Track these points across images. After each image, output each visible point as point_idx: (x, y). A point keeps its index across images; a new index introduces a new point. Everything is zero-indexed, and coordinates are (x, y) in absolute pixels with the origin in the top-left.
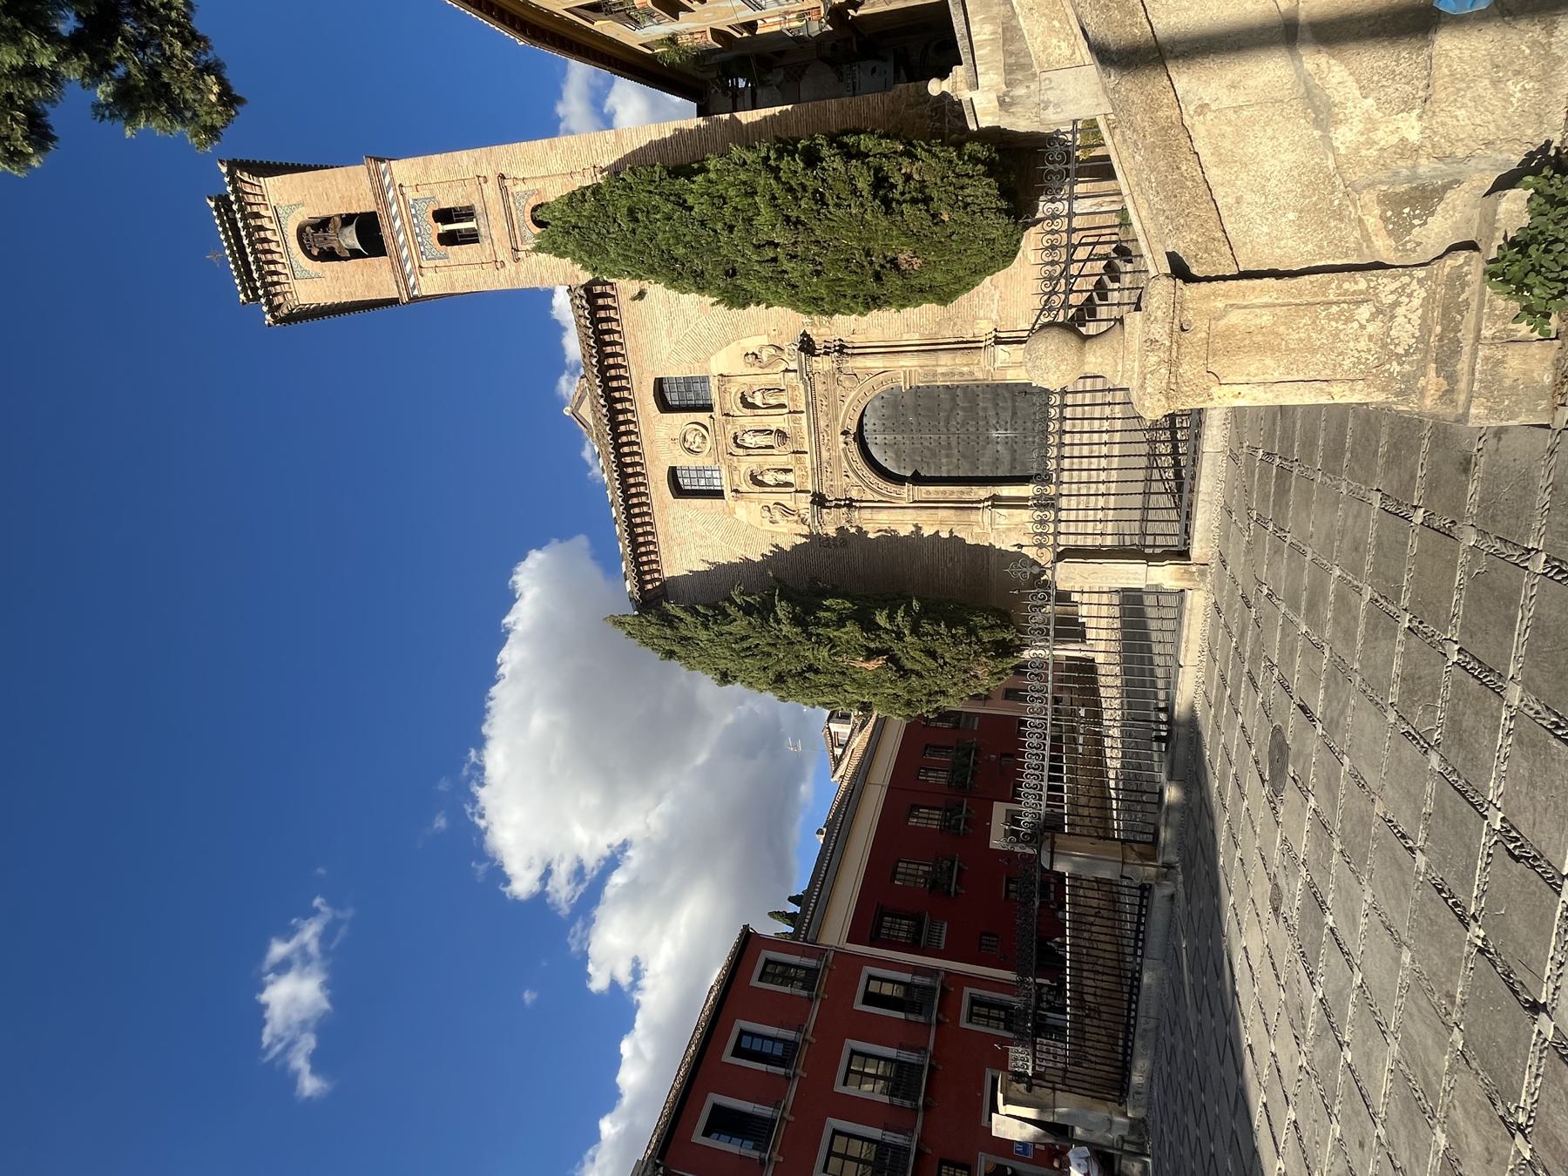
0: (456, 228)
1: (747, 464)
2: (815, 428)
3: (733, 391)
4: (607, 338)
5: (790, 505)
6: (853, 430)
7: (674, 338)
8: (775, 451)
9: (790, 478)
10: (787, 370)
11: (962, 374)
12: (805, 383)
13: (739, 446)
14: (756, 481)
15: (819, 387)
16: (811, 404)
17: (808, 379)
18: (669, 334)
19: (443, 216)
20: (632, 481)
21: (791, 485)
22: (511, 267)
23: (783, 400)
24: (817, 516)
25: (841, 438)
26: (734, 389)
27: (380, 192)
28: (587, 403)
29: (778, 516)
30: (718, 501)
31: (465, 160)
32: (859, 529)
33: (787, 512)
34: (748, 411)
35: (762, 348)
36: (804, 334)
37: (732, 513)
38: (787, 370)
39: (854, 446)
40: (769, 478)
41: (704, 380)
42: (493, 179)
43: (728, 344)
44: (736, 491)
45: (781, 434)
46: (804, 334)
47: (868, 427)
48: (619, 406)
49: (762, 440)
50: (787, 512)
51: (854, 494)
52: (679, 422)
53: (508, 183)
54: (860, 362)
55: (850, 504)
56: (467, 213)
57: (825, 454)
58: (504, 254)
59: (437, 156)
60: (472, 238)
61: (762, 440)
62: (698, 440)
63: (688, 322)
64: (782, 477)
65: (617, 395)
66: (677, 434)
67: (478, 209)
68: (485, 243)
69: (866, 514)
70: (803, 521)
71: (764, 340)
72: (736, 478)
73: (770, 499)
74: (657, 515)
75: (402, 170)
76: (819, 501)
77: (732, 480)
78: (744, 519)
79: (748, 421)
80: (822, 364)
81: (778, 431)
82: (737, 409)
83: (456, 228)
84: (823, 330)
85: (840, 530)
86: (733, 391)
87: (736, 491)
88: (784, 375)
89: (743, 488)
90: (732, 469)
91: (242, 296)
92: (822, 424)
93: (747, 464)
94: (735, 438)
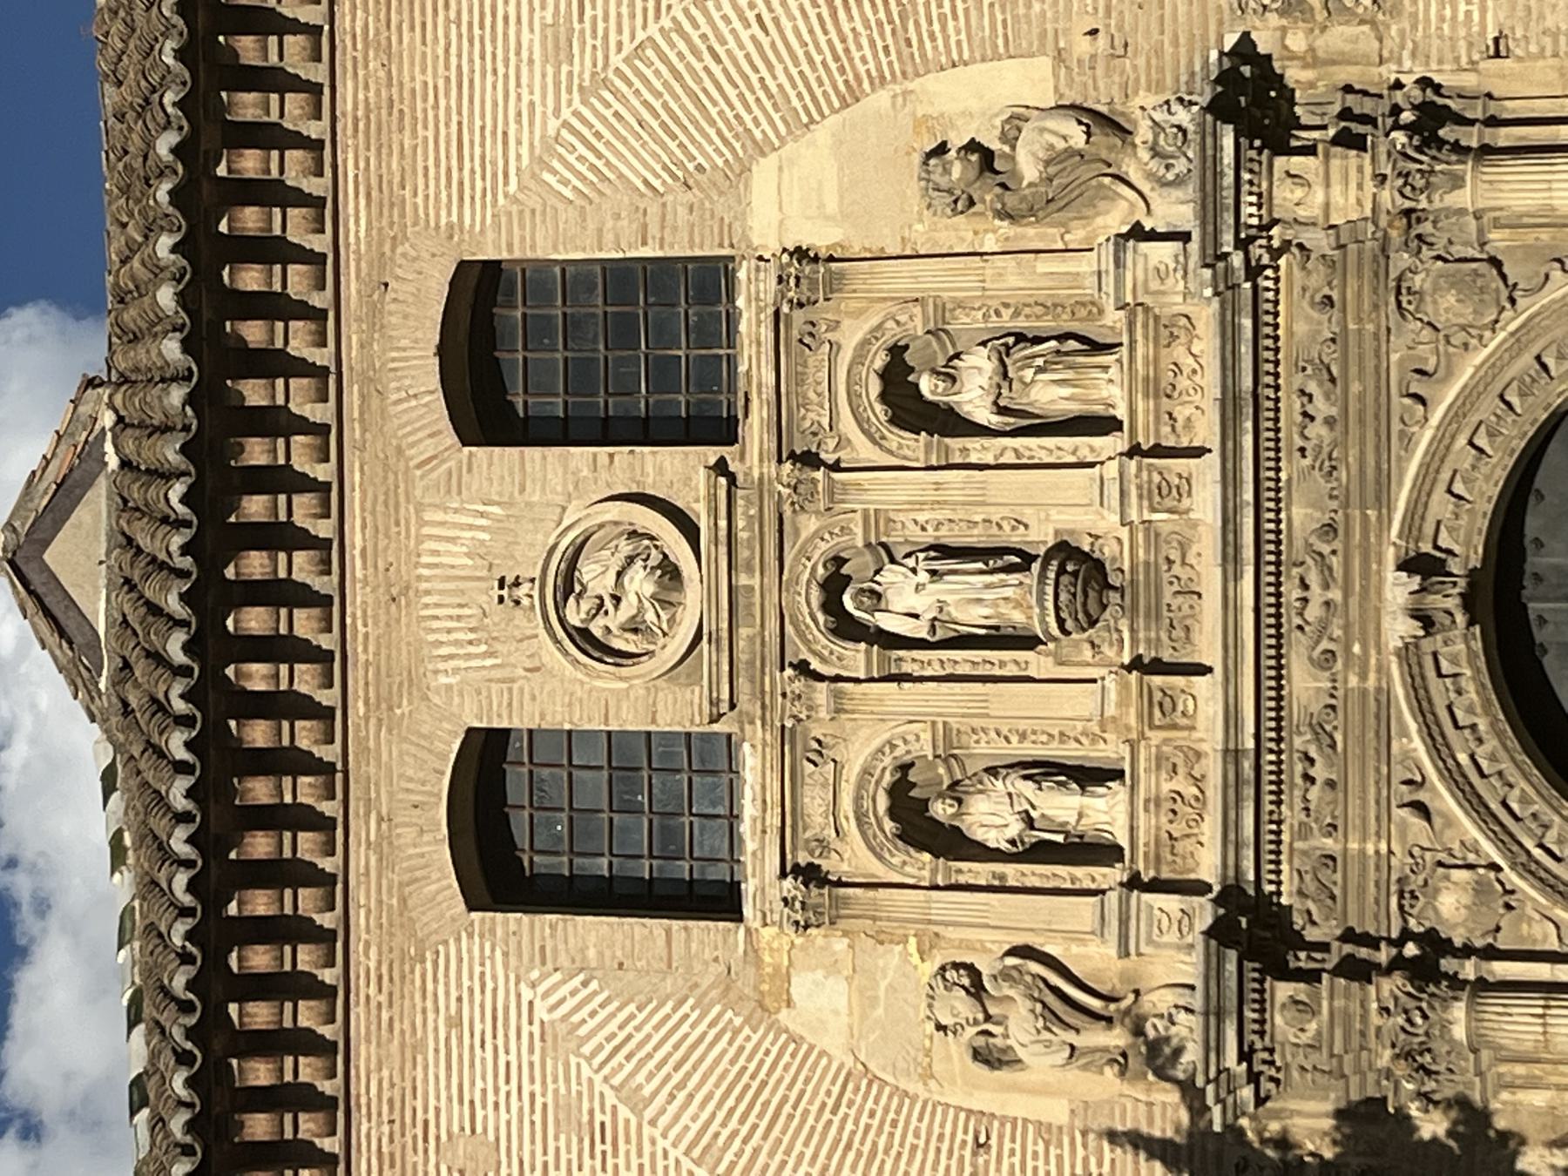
1: (883, 724)
2: (1261, 549)
3: (851, 336)
4: (247, 48)
5: (1093, 957)
6: (1465, 543)
7: (582, 66)
8: (1036, 662)
9: (1103, 812)
10: (1138, 233)
12: (1225, 289)
13: (847, 628)
14: (918, 819)
15: (1299, 323)
16: (1249, 404)
17: (1242, 257)
18: (560, 47)
20: (259, 790)
21: (1106, 853)
23: (1107, 388)
24: (1231, 1010)
25: (1398, 589)
26: (854, 332)
28: (94, 513)
29: (1019, 1025)
30: (703, 934)
32: (1472, 1117)
33: (1067, 999)
34: (915, 445)
35: (1014, 124)
36: (1245, 49)
37: (768, 1000)
38: (1138, 233)
39: (1461, 648)
40: (991, 817)
41: (709, 280)
43: (852, 96)
44: (811, 875)
45: (1080, 572)
46: (1245, 49)
47: (1553, 551)
48: (254, 393)
49: (974, 599)
50: (1067, 999)
51: (1451, 907)
52: (563, 489)
54: (1517, 189)
55: (1429, 962)
57: (1305, 685)
61: (974, 599)
62: (640, 583)
64: (1062, 807)
65: (253, 332)
66: (530, 557)
69: (1517, 1023)
70: (1157, 1057)
71: (1029, 81)
72: (815, 803)
73: (985, 924)
74: (366, 957)
76: (1253, 933)
77: (791, 819)
78: (833, 1042)
79: (907, 490)
80: (1323, 193)
81: (1064, 551)
82: (854, 429)
84: (1339, 37)
85: (1367, 1121)
86: (851, 336)
87: (811, 875)
88: (1130, 257)
89: (852, 857)
90: (796, 749)
92: (1301, 516)
93: (883, 724)
94: (834, 585)
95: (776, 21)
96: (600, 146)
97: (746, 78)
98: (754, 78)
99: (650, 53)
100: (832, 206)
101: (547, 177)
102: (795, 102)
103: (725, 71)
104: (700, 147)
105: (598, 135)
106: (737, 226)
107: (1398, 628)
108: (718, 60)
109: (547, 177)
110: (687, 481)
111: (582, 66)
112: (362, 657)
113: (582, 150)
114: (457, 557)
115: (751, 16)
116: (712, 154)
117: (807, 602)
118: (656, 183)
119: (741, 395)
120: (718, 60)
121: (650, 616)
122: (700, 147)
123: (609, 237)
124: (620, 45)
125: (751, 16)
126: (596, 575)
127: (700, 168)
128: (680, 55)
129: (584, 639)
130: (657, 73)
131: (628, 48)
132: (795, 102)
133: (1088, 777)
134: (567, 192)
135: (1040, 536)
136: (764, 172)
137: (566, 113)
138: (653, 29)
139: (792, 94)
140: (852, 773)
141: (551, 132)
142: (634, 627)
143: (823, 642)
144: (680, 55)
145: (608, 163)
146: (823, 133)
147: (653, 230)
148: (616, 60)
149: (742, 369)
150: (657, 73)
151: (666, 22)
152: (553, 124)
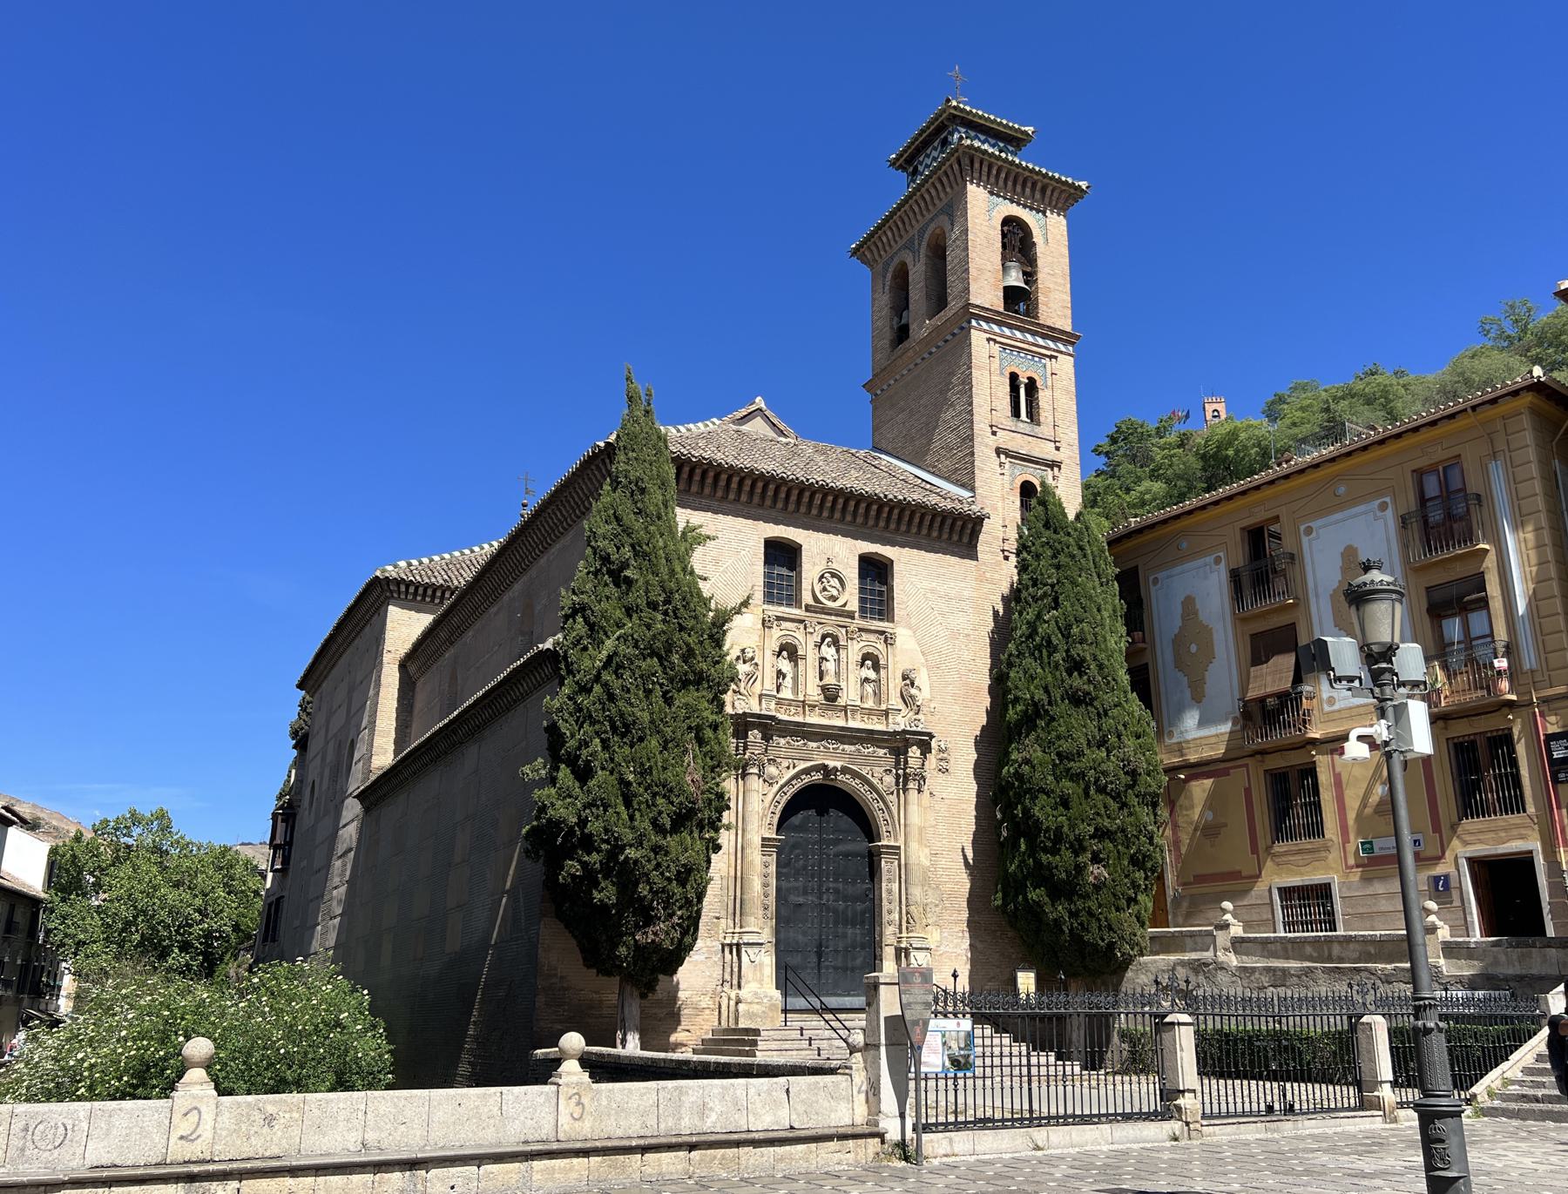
0: (1024, 396)
11: (890, 912)
13: (824, 637)
18: (933, 591)
19: (1032, 386)
22: (993, 442)
27: (1052, 334)
31: (1070, 434)
42: (1056, 456)
56: (1033, 415)
58: (1004, 439)
60: (1016, 413)
62: (835, 593)
67: (1037, 430)
68: (1010, 423)
75: (1065, 366)
83: (1024, 396)
91: (954, 103)
93: (807, 644)
107: (831, 764)
114: (837, 549)
116: (913, 621)
117: (829, 629)
126: (835, 582)
133: (795, 689)
135: (843, 684)
136: (910, 632)
142: (825, 589)
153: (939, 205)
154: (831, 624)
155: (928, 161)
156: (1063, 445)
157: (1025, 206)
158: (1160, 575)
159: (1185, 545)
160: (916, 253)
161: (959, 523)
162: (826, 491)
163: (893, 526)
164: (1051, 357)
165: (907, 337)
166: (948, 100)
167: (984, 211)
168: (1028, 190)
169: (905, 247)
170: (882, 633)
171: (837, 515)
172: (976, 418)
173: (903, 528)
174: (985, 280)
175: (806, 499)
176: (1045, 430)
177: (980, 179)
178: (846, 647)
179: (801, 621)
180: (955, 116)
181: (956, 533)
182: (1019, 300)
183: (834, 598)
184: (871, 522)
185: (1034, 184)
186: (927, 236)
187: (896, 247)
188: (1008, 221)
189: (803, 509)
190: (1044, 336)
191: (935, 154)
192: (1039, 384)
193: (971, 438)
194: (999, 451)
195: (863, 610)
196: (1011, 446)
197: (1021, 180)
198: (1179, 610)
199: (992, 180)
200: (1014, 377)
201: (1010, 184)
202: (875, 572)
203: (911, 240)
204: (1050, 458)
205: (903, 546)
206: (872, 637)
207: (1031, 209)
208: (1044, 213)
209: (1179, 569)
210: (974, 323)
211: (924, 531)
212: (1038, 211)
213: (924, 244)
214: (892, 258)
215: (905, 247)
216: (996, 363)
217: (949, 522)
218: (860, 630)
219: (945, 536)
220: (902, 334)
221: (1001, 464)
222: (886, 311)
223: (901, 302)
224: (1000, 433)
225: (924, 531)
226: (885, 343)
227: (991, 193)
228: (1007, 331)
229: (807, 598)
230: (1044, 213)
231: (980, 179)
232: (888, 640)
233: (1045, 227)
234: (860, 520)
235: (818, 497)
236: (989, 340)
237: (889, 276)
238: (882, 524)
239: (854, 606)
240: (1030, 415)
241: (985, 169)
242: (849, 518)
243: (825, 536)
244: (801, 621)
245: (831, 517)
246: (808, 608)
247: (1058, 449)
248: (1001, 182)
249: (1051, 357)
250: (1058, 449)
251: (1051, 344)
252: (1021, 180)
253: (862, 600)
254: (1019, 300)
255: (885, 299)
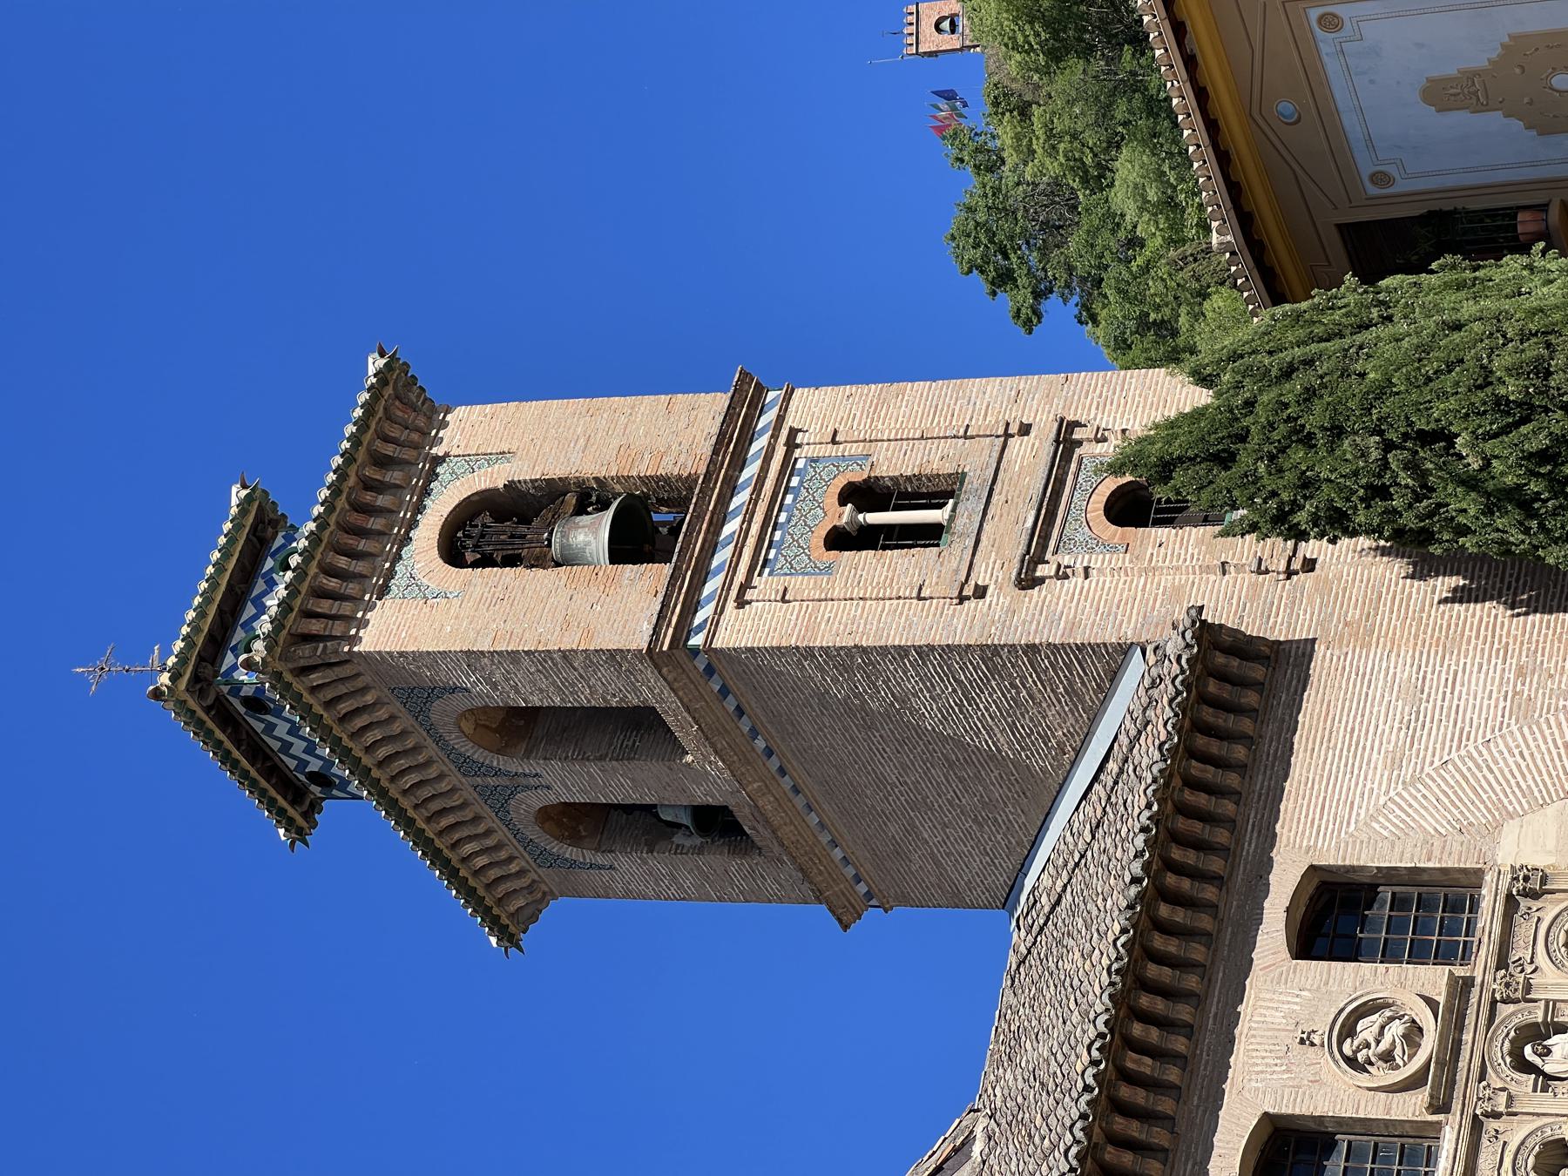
0: (887, 513)
7: (1407, 772)
18: (1396, 763)
19: (863, 494)
22: (1002, 596)
27: (733, 441)
31: (988, 399)
42: (1045, 431)
53: (1078, 434)
56: (937, 492)
59: (920, 385)
60: (930, 535)
62: (1396, 1029)
63: (1461, 738)
67: (976, 481)
68: (954, 552)
75: (816, 411)
83: (887, 513)
91: (165, 679)
95: (1532, 755)
96: (1410, 811)
97: (1508, 781)
98: (1513, 782)
99: (1450, 767)
100: (1551, 844)
101: (1374, 825)
102: (1537, 794)
103: (1496, 778)
104: (1473, 813)
105: (1410, 806)
106: (1489, 854)
108: (1492, 771)
109: (1374, 825)
110: (1434, 985)
111: (1407, 772)
112: (1202, 1072)
113: (1398, 812)
114: (1277, 1018)
115: (1516, 752)
116: (1480, 817)
117: (1500, 1051)
118: (1443, 831)
119: (1476, 940)
120: (1492, 771)
121: (1398, 1052)
122: (1473, 813)
123: (1407, 856)
124: (1432, 763)
125: (1516, 752)
126: (1367, 1028)
127: (1471, 824)
128: (1469, 769)
129: (1351, 1062)
130: (1453, 777)
131: (1437, 763)
132: (1537, 794)
134: (1385, 833)
136: (1510, 830)
137: (1392, 793)
138: (1454, 755)
139: (1535, 790)
140: (1512, 1148)
141: (1382, 802)
142: (1387, 1057)
143: (1507, 1071)
144: (1469, 769)
145: (1414, 820)
146: (1551, 810)
147: (1436, 853)
148: (1427, 769)
149: (1480, 925)
150: (1453, 777)
151: (1463, 752)
152: (1382, 800)
153: (405, 721)
154: (1485, 1045)
155: (298, 747)
156: (1016, 416)
157: (419, 508)
158: (1366, 168)
159: (1286, 107)
160: (517, 784)
161: (1212, 687)
162: (1118, 1042)
163: (1215, 864)
164: (791, 445)
165: (724, 810)
166: (157, 694)
167: (427, 611)
168: (382, 501)
169: (502, 810)
170: (1511, 903)
171: (1183, 1012)
172: (939, 638)
173: (1221, 836)
174: (587, 609)
175: (1139, 1097)
176: (975, 461)
177: (349, 619)
178: (1551, 1006)
179: (1477, 1125)
180: (196, 678)
181: (1238, 696)
182: (646, 525)
183: (1414, 1033)
184: (1205, 922)
185: (368, 485)
186: (479, 755)
187: (502, 833)
188: (453, 552)
189: (1165, 1105)
190: (739, 462)
191: (282, 730)
192: (858, 475)
193: (990, 653)
194: (1027, 581)
195: (1445, 955)
196: (1015, 549)
197: (356, 518)
198: (1460, 120)
199: (352, 588)
200: (839, 540)
201: (363, 545)
202: (1340, 915)
203: (487, 793)
204: (1047, 449)
205: (1270, 839)
206: (1523, 930)
207: (426, 492)
208: (438, 461)
209: (1349, 121)
210: (697, 640)
211: (1232, 780)
212: (432, 476)
213: (498, 761)
214: (528, 844)
215: (502, 810)
216: (800, 585)
217: (1208, 714)
218: (1502, 963)
219: (1246, 725)
220: (716, 824)
221: (1062, 575)
222: (658, 863)
223: (639, 824)
224: (980, 577)
225: (1232, 780)
226: (736, 866)
227: (383, 591)
228: (722, 556)
229: (1412, 1107)
230: (438, 461)
231: (349, 619)
232: (1530, 887)
233: (473, 460)
234: (1197, 952)
235: (1132, 1061)
236: (741, 603)
237: (570, 852)
238: (1209, 893)
239: (1434, 979)
240: (935, 499)
241: (325, 606)
242: (1192, 982)
243: (1240, 1048)
244: (1477, 1125)
245: (1188, 1030)
246: (1441, 1105)
247: (1025, 430)
248: (359, 567)
249: (791, 445)
250: (1025, 430)
251: (760, 444)
252: (356, 518)
253: (1419, 955)
254: (646, 525)
255: (628, 866)
